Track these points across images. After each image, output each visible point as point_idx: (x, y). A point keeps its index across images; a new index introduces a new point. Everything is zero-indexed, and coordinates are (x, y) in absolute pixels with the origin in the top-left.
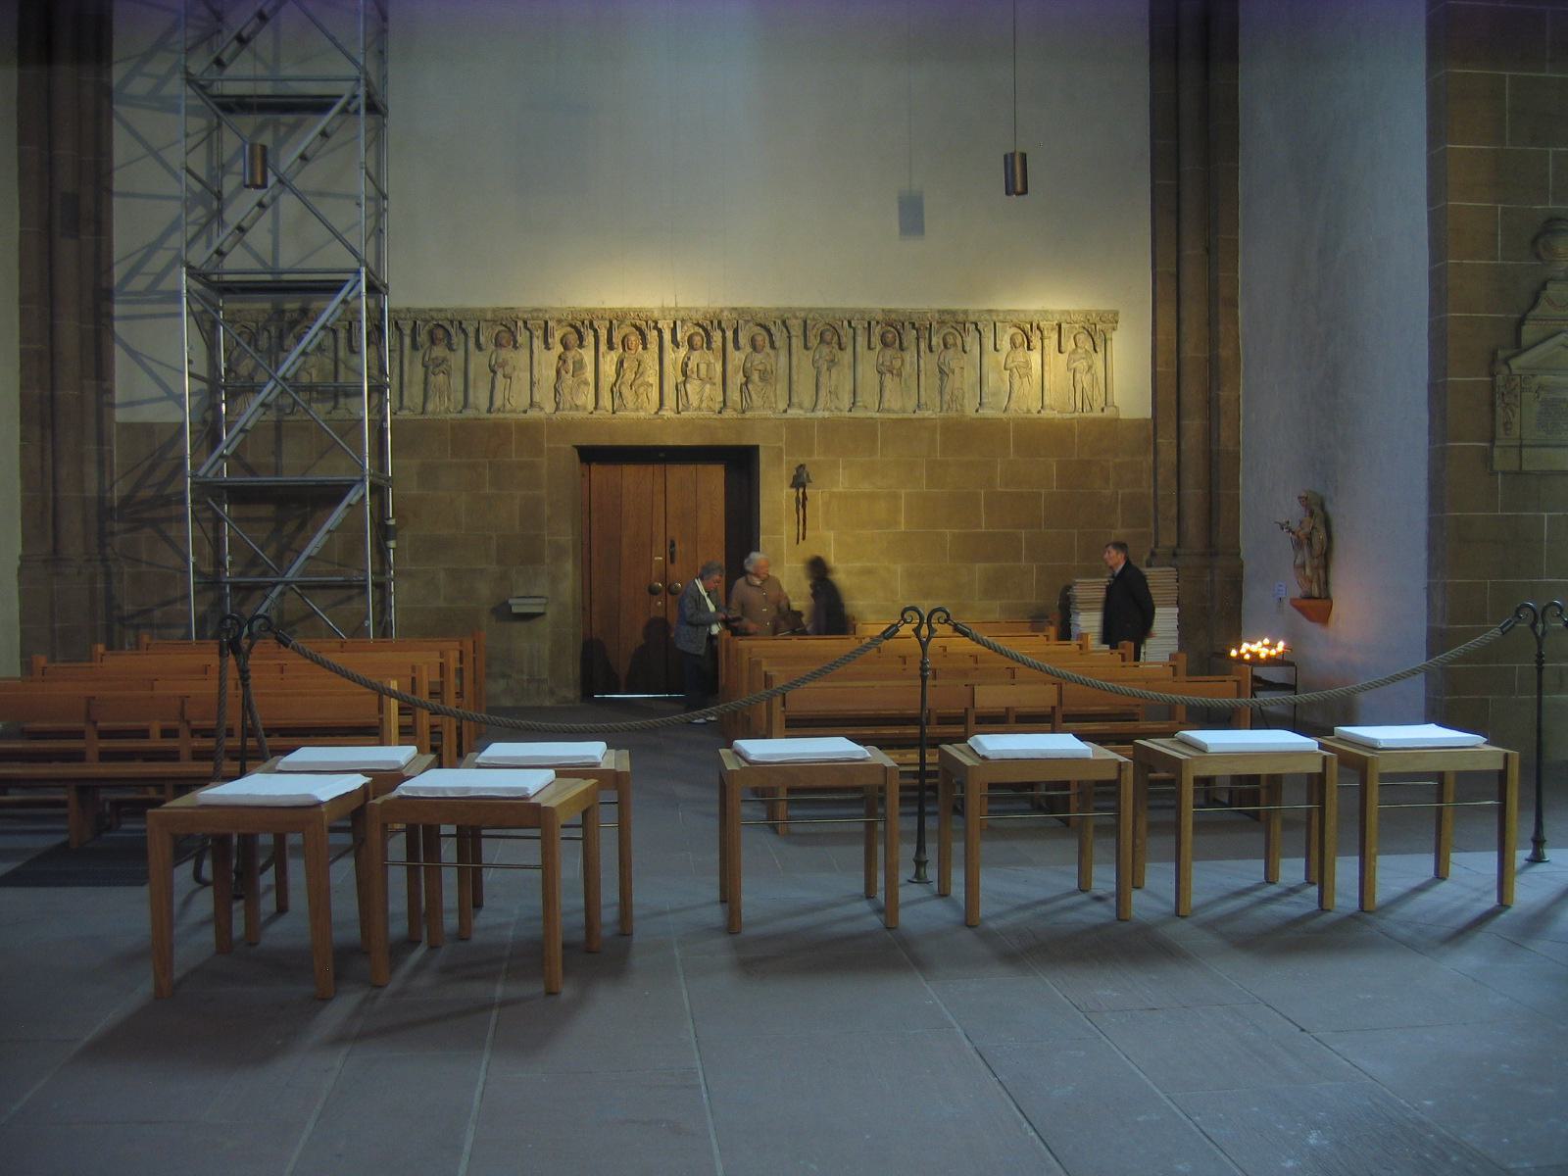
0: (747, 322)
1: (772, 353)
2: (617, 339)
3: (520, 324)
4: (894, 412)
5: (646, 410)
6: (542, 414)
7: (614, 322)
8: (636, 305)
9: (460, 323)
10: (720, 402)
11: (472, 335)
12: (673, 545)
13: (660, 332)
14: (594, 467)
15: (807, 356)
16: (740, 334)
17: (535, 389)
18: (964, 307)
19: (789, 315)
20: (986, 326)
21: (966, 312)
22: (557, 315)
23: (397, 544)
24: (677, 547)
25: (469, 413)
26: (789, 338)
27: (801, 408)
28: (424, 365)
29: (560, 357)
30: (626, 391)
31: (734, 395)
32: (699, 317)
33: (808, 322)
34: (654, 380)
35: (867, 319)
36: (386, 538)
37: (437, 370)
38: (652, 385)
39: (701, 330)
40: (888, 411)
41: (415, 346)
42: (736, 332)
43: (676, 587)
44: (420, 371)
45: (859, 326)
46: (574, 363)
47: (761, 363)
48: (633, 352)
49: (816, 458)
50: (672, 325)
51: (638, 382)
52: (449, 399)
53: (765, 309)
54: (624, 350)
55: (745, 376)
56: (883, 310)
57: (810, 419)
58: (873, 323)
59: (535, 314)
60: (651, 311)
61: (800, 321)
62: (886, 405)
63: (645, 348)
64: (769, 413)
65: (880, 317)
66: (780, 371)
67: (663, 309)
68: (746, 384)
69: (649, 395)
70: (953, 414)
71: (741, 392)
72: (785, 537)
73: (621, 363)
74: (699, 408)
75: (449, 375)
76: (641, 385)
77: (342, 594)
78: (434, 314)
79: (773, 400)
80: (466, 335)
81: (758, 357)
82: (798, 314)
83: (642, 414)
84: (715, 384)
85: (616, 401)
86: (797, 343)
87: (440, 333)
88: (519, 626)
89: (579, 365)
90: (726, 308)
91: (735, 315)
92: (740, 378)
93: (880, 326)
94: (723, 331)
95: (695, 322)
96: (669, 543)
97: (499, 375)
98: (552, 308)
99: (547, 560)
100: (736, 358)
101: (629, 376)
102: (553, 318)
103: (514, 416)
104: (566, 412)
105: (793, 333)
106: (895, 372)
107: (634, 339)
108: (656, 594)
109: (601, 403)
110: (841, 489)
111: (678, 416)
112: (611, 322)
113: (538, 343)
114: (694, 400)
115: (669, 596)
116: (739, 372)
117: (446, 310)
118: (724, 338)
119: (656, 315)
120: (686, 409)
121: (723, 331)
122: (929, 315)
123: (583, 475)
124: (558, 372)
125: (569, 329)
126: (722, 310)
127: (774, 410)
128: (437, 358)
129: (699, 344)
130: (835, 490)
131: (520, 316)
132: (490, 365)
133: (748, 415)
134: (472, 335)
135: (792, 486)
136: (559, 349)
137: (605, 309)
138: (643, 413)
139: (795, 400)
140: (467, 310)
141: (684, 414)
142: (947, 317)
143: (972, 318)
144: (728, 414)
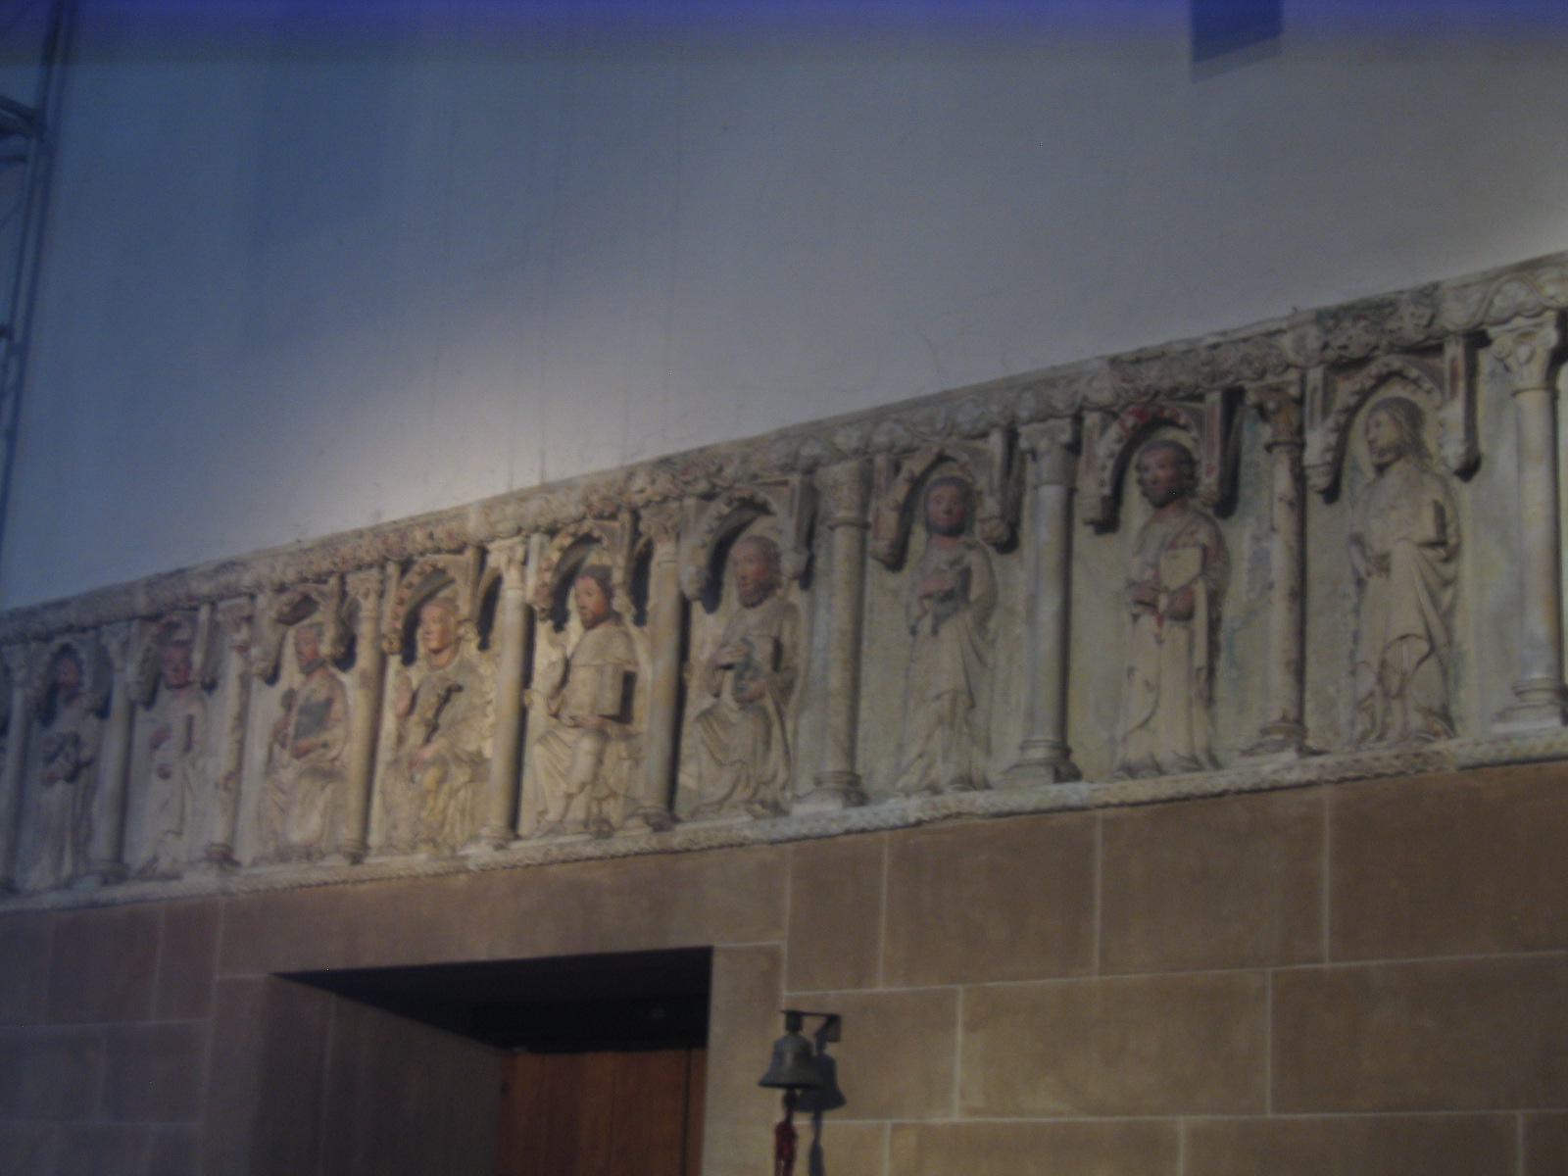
4: (1159, 769)
18: (1425, 279)
20: (1525, 335)
21: (1429, 295)
32: (568, 507)
35: (1060, 399)
38: (477, 761)
40: (1130, 771)
45: (1043, 444)
49: (880, 988)
56: (1114, 361)
57: (863, 831)
58: (1091, 419)
60: (459, 514)
61: (853, 464)
62: (1134, 753)
63: (484, 646)
64: (740, 824)
65: (1102, 391)
67: (489, 506)
70: (1381, 755)
74: (556, 829)
89: (319, 715)
90: (642, 465)
91: (663, 484)
93: (1114, 431)
106: (1163, 602)
110: (957, 1118)
119: (474, 527)
122: (1286, 342)
126: (631, 474)
130: (937, 1120)
133: (679, 836)
142: (1355, 337)
143: (1456, 315)
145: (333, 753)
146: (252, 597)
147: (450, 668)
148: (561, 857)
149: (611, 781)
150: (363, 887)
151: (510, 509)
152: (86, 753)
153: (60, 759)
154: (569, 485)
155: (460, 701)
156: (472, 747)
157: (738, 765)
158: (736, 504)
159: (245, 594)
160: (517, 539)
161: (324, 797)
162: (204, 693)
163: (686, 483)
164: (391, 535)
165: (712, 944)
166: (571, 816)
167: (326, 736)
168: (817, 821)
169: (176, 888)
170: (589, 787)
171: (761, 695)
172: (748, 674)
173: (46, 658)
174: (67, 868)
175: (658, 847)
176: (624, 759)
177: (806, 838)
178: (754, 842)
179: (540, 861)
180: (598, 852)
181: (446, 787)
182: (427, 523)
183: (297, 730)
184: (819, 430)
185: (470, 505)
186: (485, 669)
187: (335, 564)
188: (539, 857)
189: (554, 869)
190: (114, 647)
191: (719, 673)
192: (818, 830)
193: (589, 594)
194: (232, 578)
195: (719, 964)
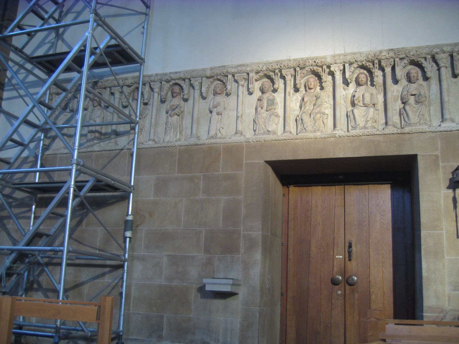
0: (401, 59)
1: (424, 83)
2: (301, 82)
3: (230, 76)
5: (321, 132)
6: (241, 139)
7: (298, 69)
8: (314, 55)
9: (190, 81)
10: (383, 124)
11: (197, 87)
12: (350, 246)
13: (332, 74)
14: (292, 188)
15: (455, 83)
16: (397, 69)
17: (239, 122)
19: (438, 50)
22: (255, 68)
23: (133, 234)
24: (354, 248)
25: (193, 141)
26: (439, 70)
27: (452, 121)
28: (167, 113)
29: (258, 100)
30: (306, 118)
31: (395, 118)
32: (361, 58)
33: (455, 54)
34: (329, 112)
36: (125, 230)
37: (173, 112)
38: (327, 114)
39: (365, 72)
41: (163, 102)
42: (393, 69)
43: (353, 279)
44: (164, 115)
46: (267, 101)
47: (416, 89)
48: (312, 91)
50: (342, 68)
51: (317, 110)
52: (181, 133)
53: (418, 48)
54: (306, 91)
55: (403, 103)
59: (240, 69)
60: (325, 58)
61: (447, 54)
63: (322, 88)
64: (425, 128)
66: (433, 97)
67: (334, 56)
68: (404, 108)
69: (325, 121)
71: (400, 115)
72: (444, 232)
73: (303, 99)
74: (365, 127)
75: (182, 118)
76: (318, 113)
77: (100, 271)
78: (173, 76)
79: (428, 119)
80: (193, 88)
81: (413, 88)
82: (445, 49)
83: (318, 134)
84: (378, 110)
85: (300, 127)
86: (446, 73)
87: (177, 89)
88: (219, 303)
89: (272, 102)
90: (384, 50)
91: (392, 54)
92: (399, 105)
94: (382, 69)
95: (361, 64)
96: (347, 245)
97: (214, 113)
98: (252, 64)
99: (242, 250)
100: (394, 90)
101: (309, 107)
102: (252, 70)
103: (222, 141)
104: (260, 136)
105: (442, 64)
107: (313, 80)
108: (337, 285)
109: (287, 127)
111: (348, 134)
112: (295, 70)
113: (243, 90)
114: (361, 122)
115: (347, 287)
116: (398, 99)
117: (180, 72)
118: (384, 76)
119: (329, 60)
120: (354, 128)
121: (382, 69)
123: (284, 195)
124: (256, 109)
125: (266, 80)
126: (381, 52)
127: (430, 126)
128: (173, 105)
129: (364, 80)
131: (229, 70)
132: (209, 109)
134: (197, 87)
135: (448, 188)
136: (257, 94)
137: (290, 60)
138: (320, 133)
139: (447, 116)
140: (193, 71)
141: (353, 132)
144: (390, 130)
145: (276, 111)
146: (248, 74)
147: (315, 93)
148: (368, 134)
149: (375, 119)
150: (298, 140)
151: (341, 57)
152: (182, 109)
153: (177, 110)
154: (361, 53)
155: (319, 100)
156: (323, 111)
157: (422, 115)
158: (409, 61)
159: (246, 72)
160: (342, 64)
161: (276, 120)
162: (226, 97)
163: (399, 55)
164: (301, 61)
165: (417, 154)
166: (367, 126)
167: (275, 107)
168: (449, 128)
169: (228, 140)
170: (372, 119)
171: (424, 101)
172: (420, 97)
173: (169, 86)
174: (178, 137)
175: (399, 132)
176: (377, 114)
177: (445, 131)
178: (429, 132)
179: (361, 135)
180: (380, 133)
181: (321, 119)
182: (313, 59)
183: (268, 104)
184: (437, 46)
185: (328, 56)
186: (323, 94)
187: (281, 67)
188: (361, 134)
189: (364, 137)
190: (196, 84)
191: (410, 96)
192: (449, 129)
193: (364, 78)
194: (244, 68)
195: (419, 158)
